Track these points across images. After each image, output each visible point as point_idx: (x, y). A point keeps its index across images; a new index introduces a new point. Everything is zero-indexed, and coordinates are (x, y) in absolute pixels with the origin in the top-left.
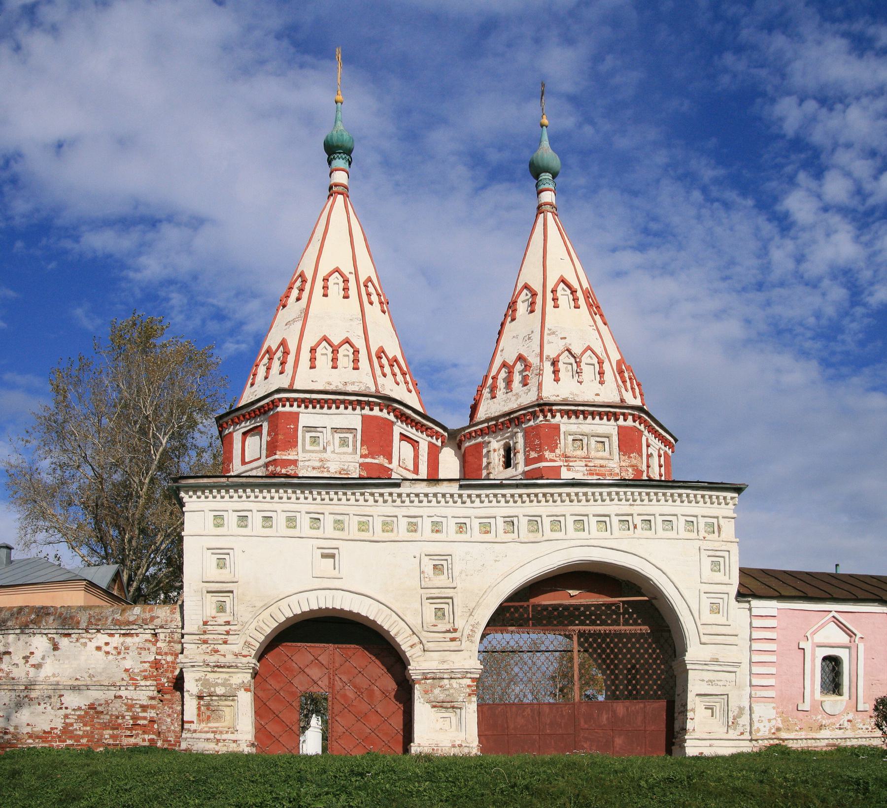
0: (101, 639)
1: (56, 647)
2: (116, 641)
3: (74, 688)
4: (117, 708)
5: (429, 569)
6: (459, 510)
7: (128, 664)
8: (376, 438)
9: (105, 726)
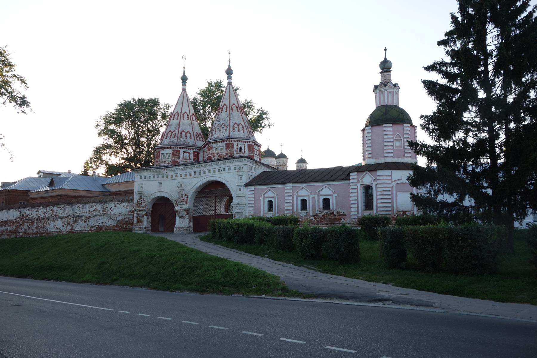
0: (124, 204)
1: (115, 206)
2: (127, 204)
3: (119, 215)
4: (127, 219)
5: (180, 186)
6: (185, 171)
7: (128, 210)
8: (176, 154)
9: (124, 224)
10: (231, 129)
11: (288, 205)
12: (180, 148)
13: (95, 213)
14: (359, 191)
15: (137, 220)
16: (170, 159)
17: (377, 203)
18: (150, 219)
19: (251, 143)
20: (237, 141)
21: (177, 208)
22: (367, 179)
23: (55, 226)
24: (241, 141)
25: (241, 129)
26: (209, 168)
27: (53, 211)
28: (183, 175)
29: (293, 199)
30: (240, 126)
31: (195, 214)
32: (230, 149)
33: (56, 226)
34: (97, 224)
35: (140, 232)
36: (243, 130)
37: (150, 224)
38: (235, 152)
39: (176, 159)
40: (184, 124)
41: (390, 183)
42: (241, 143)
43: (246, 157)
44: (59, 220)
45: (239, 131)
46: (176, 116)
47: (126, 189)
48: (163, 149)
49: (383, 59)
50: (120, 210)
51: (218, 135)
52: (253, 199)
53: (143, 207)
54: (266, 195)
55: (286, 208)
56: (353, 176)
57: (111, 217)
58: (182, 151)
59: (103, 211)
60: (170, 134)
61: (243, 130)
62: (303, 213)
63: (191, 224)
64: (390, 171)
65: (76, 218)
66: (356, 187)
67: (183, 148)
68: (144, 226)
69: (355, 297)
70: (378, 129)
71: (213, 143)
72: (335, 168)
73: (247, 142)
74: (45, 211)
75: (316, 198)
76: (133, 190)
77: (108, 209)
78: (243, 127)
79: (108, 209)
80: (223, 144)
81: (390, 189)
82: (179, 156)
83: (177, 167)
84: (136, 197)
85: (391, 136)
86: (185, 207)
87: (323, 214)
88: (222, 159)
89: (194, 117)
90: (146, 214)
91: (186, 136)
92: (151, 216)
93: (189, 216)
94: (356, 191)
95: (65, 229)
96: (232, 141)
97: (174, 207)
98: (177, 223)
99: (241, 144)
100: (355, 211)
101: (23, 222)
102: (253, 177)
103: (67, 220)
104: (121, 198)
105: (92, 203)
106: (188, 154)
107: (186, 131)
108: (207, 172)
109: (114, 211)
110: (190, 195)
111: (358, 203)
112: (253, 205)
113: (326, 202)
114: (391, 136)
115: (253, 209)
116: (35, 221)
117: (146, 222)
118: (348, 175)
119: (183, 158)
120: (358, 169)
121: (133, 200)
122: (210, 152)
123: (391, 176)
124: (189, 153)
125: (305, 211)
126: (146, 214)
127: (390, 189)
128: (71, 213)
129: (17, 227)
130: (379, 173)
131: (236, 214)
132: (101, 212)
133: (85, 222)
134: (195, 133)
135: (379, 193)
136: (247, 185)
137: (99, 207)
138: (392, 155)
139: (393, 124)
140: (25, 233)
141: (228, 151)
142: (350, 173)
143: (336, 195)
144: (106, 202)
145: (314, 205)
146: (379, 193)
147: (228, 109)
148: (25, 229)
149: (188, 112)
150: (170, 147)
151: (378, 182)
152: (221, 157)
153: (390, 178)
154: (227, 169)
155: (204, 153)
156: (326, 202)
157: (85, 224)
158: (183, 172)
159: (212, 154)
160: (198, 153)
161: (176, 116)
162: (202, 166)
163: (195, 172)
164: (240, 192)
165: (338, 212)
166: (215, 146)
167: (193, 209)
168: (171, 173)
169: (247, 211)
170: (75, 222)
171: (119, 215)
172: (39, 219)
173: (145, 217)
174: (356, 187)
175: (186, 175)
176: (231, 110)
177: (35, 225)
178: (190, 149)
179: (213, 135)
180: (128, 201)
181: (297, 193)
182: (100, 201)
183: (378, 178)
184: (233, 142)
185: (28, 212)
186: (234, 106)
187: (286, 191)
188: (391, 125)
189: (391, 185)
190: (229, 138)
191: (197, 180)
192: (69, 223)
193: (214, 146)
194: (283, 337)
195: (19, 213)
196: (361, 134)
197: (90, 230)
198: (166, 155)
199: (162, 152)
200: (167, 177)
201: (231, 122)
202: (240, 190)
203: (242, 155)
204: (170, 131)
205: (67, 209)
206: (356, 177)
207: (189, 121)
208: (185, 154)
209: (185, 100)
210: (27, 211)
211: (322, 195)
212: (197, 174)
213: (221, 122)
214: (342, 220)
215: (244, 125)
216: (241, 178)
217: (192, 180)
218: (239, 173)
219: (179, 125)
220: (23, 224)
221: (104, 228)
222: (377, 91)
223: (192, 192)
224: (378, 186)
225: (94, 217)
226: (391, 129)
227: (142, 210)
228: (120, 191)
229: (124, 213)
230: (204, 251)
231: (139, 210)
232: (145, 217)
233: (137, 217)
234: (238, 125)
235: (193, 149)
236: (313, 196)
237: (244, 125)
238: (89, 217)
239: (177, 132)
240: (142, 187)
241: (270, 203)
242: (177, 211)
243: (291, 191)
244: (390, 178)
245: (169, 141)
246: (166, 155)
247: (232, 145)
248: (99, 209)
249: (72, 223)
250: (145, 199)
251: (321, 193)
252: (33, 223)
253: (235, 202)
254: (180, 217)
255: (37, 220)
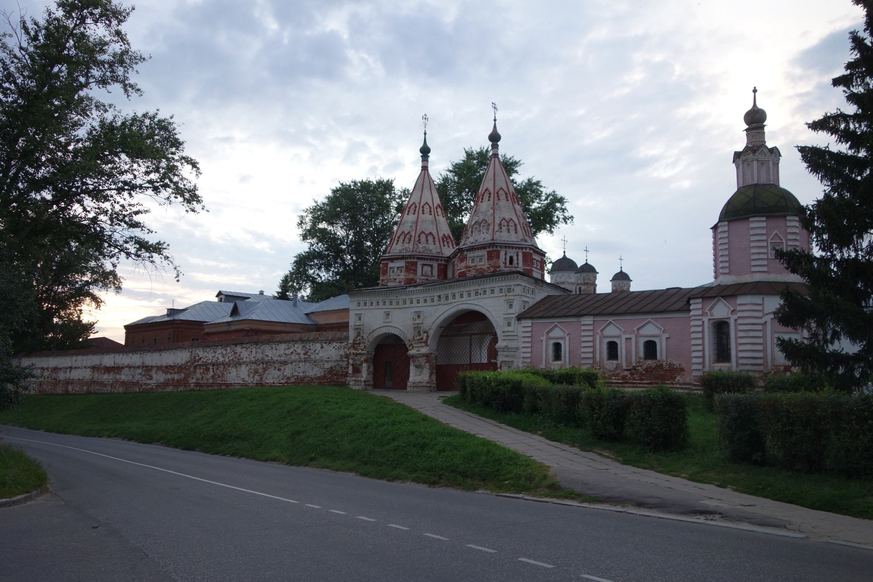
0: (335, 344)
1: (322, 347)
2: (338, 345)
3: (327, 362)
4: (338, 368)
5: (416, 317)
7: (341, 353)
8: (411, 267)
9: (335, 375)
10: (497, 228)
11: (586, 352)
12: (418, 258)
13: (293, 357)
14: (706, 330)
15: (353, 368)
16: (402, 276)
17: (737, 351)
18: (372, 369)
19: (528, 250)
20: (506, 247)
21: (412, 352)
22: (721, 310)
23: (237, 376)
24: (513, 248)
25: (512, 228)
26: (462, 289)
27: (236, 353)
28: (422, 301)
29: (594, 341)
30: (511, 224)
31: (441, 362)
32: (495, 260)
33: (238, 376)
34: (296, 374)
35: (357, 388)
36: (516, 229)
37: (371, 376)
38: (502, 265)
39: (411, 276)
40: (424, 221)
41: (761, 318)
42: (511, 250)
43: (519, 272)
44: (243, 366)
45: (508, 231)
46: (412, 211)
47: (340, 321)
48: (392, 260)
49: (749, 107)
50: (329, 353)
51: (476, 238)
52: (530, 340)
53: (362, 350)
54: (551, 335)
55: (583, 356)
56: (696, 306)
57: (315, 362)
58: (420, 263)
59: (305, 354)
60: (402, 237)
61: (516, 229)
62: (611, 365)
63: (434, 377)
64: (760, 297)
65: (267, 364)
66: (700, 323)
67: (422, 259)
68: (363, 379)
69: (661, 505)
70: (739, 227)
71: (467, 250)
72: (668, 289)
73: (522, 248)
74: (224, 352)
75: (634, 339)
76: (348, 323)
77: (312, 351)
78: (515, 225)
79: (312, 351)
80: (484, 253)
81: (760, 327)
82: (415, 270)
83: (412, 289)
84: (352, 334)
85: (765, 238)
86: (424, 350)
87: (645, 367)
88: (481, 276)
89: (439, 210)
90: (366, 361)
91: (427, 240)
92: (374, 364)
93: (431, 366)
94: (700, 329)
95: (252, 380)
96: (497, 247)
97: (407, 350)
98: (411, 375)
99: (511, 252)
100: (699, 364)
101: (195, 367)
102: (531, 304)
103: (254, 366)
104: (330, 335)
105: (289, 342)
106: (429, 269)
107: (427, 233)
108: (458, 295)
109: (320, 355)
110: (431, 333)
111: (703, 350)
112: (529, 350)
113: (650, 348)
114: (765, 238)
115: (529, 355)
116: (211, 367)
117: (365, 373)
118: (688, 303)
119: (422, 275)
120: (705, 294)
121: (347, 338)
122: (464, 264)
123: (762, 305)
124: (431, 266)
125: (615, 362)
126: (366, 361)
127: (760, 327)
128: (259, 356)
129: (187, 376)
130: (741, 300)
131: (503, 365)
132: (302, 356)
133: (279, 370)
134: (441, 235)
135: (740, 334)
136: (520, 318)
137: (299, 348)
138: (765, 269)
139: (767, 217)
140: (197, 384)
141: (492, 262)
142: (689, 299)
143: (667, 336)
144: (308, 341)
145: (628, 352)
146: (740, 334)
147: (492, 196)
148: (198, 379)
149: (430, 203)
150: (403, 258)
151: (740, 314)
152: (481, 273)
153: (760, 308)
154: (488, 291)
155: (454, 266)
156: (650, 348)
157: (278, 373)
158: (421, 296)
159: (466, 267)
160: (446, 266)
161: (412, 211)
162: (451, 287)
163: (439, 297)
164: (510, 329)
165: (670, 365)
166: (472, 255)
167: (437, 353)
168: (404, 297)
169: (521, 360)
170: (265, 370)
171: (327, 362)
172: (216, 365)
173: (365, 365)
174: (700, 323)
175: (425, 301)
176: (496, 198)
177: (211, 373)
178: (433, 260)
179: (468, 238)
180: (340, 340)
181: (602, 331)
182: (302, 341)
183: (739, 308)
184: (499, 249)
185: (201, 354)
186: (501, 192)
187: (583, 328)
188: (764, 219)
189: (762, 321)
190: (492, 245)
191: (443, 308)
192: (256, 372)
193: (470, 255)
194: (525, 556)
195: (189, 354)
196: (711, 233)
197: (286, 383)
198: (396, 270)
199: (391, 265)
200: (398, 303)
201: (497, 217)
202: (509, 324)
203: (514, 269)
204: (403, 232)
205: (254, 350)
206: (700, 306)
207: (431, 217)
208: (425, 268)
209: (427, 184)
210: (200, 353)
211: (642, 336)
212: (443, 299)
213: (481, 218)
214: (678, 378)
215: (516, 221)
216: (511, 306)
217: (436, 310)
218: (507, 298)
219: (417, 223)
220: (195, 371)
221: (306, 380)
222: (740, 161)
223: (434, 327)
224: (739, 321)
225: (291, 363)
226: (764, 224)
227: (360, 354)
228: (332, 324)
229: (334, 358)
230: (444, 422)
231: (357, 354)
232: (365, 365)
233: (353, 365)
234: (508, 222)
235: (437, 260)
236: (628, 336)
237: (516, 221)
238: (285, 363)
239: (413, 234)
240: (360, 319)
241: (557, 347)
242: (413, 356)
243: (591, 328)
244: (760, 308)
245: (400, 248)
246: (396, 270)
247: (498, 253)
248: (299, 351)
249: (261, 371)
250: (365, 337)
251: (642, 332)
252: (208, 370)
253: (501, 344)
254: (417, 367)
255: (213, 365)
